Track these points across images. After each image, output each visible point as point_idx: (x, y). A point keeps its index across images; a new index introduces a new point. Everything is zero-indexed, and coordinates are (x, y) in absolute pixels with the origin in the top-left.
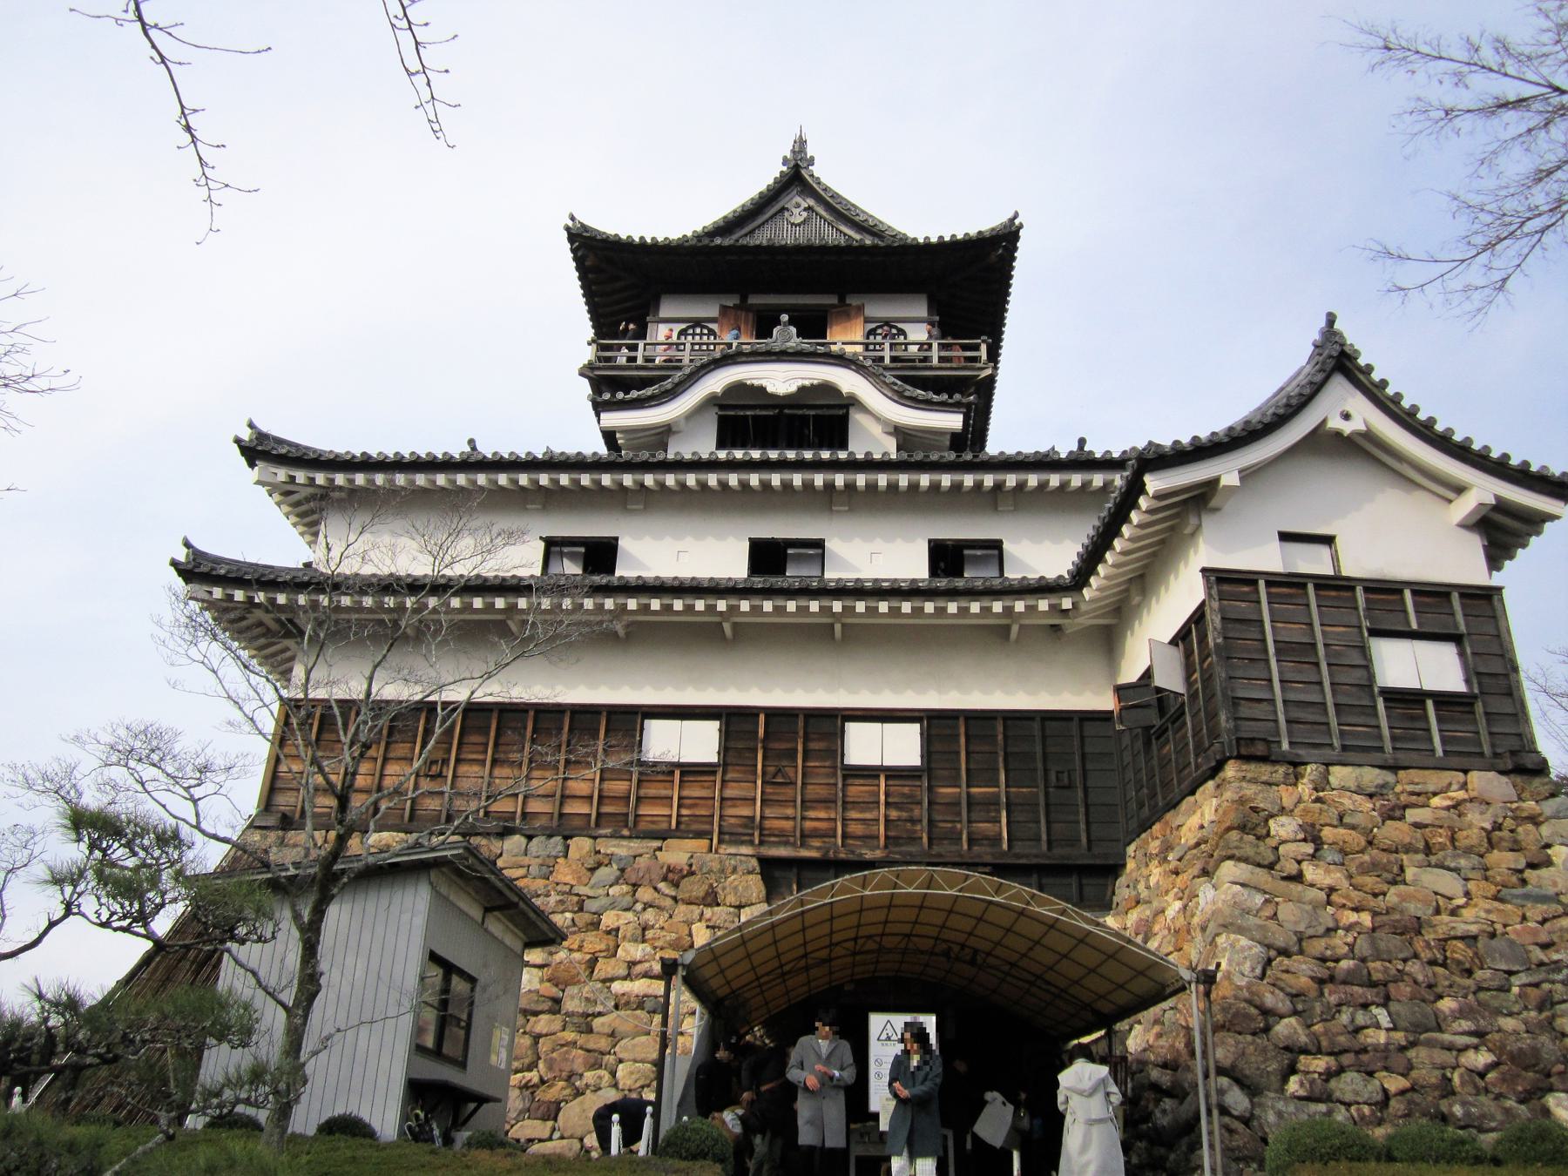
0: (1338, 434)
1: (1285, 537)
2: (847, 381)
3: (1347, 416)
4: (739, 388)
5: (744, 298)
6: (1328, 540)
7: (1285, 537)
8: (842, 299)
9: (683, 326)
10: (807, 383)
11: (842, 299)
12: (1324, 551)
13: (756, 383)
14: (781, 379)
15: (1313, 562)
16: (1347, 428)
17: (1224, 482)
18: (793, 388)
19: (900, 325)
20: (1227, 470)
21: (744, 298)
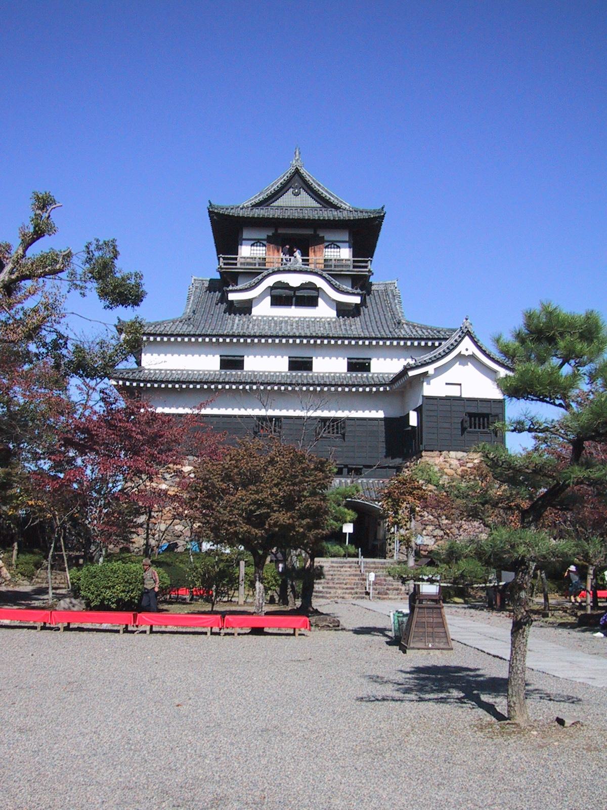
0: (464, 355)
1: (447, 384)
2: (320, 282)
3: (467, 350)
4: (279, 282)
5: (276, 230)
6: (460, 384)
7: (447, 384)
8: (315, 231)
9: (253, 242)
10: (304, 282)
11: (315, 231)
12: (459, 387)
13: (285, 282)
14: (294, 280)
15: (454, 392)
16: (467, 353)
17: (429, 373)
18: (298, 285)
19: (338, 244)
20: (430, 369)
21: (276, 230)
